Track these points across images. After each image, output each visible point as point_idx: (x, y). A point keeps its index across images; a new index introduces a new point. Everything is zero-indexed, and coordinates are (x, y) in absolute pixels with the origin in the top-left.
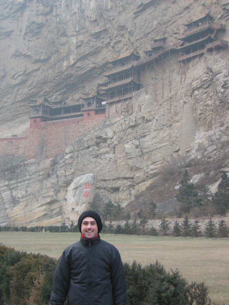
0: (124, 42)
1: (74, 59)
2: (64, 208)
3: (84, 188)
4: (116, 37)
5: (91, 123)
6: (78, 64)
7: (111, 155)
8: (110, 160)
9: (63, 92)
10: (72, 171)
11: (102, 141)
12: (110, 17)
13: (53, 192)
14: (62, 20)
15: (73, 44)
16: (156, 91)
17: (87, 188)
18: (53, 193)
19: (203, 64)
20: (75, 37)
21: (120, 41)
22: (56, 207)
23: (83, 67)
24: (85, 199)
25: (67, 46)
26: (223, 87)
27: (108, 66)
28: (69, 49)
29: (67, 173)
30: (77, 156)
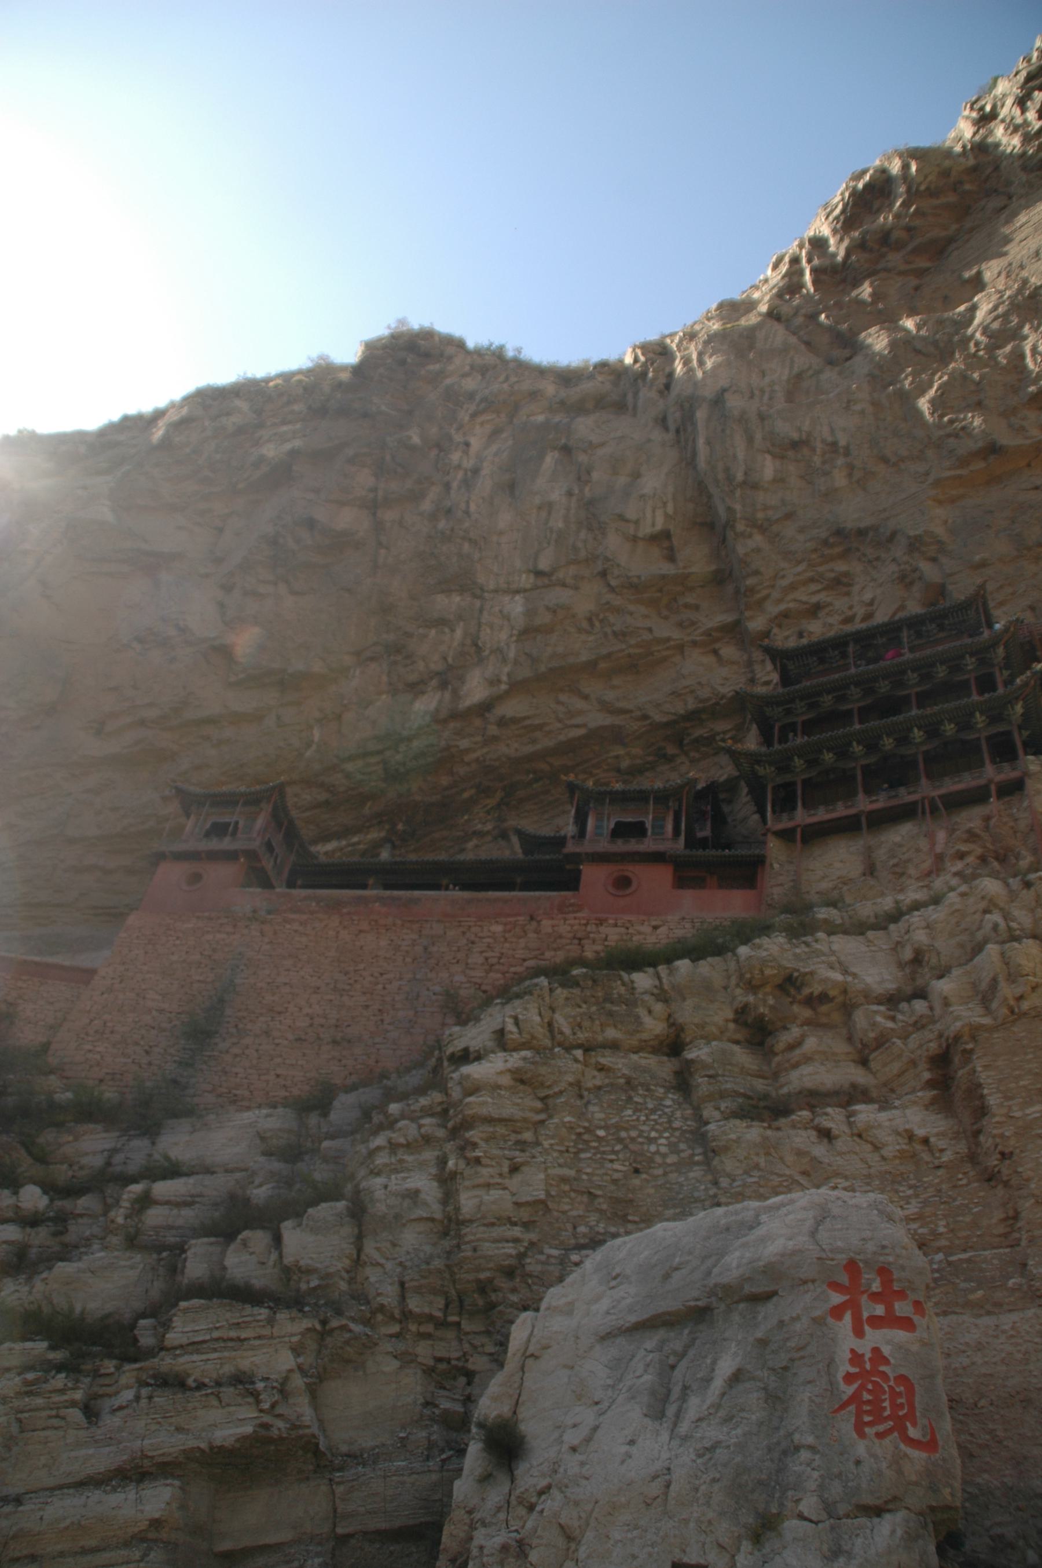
0: (851, 608)
3: (837, 1312)
4: (793, 587)
5: (646, 929)
6: (511, 708)
8: (902, 1155)
9: (361, 846)
11: (807, 1013)
12: (766, 508)
13: (297, 1350)
14: (467, 524)
15: (507, 618)
17: (876, 1322)
18: (286, 1361)
20: (517, 598)
21: (814, 611)
22: (284, 1536)
23: (537, 722)
25: (459, 633)
27: (699, 732)
28: (468, 641)
29: (467, 1202)
30: (578, 1084)
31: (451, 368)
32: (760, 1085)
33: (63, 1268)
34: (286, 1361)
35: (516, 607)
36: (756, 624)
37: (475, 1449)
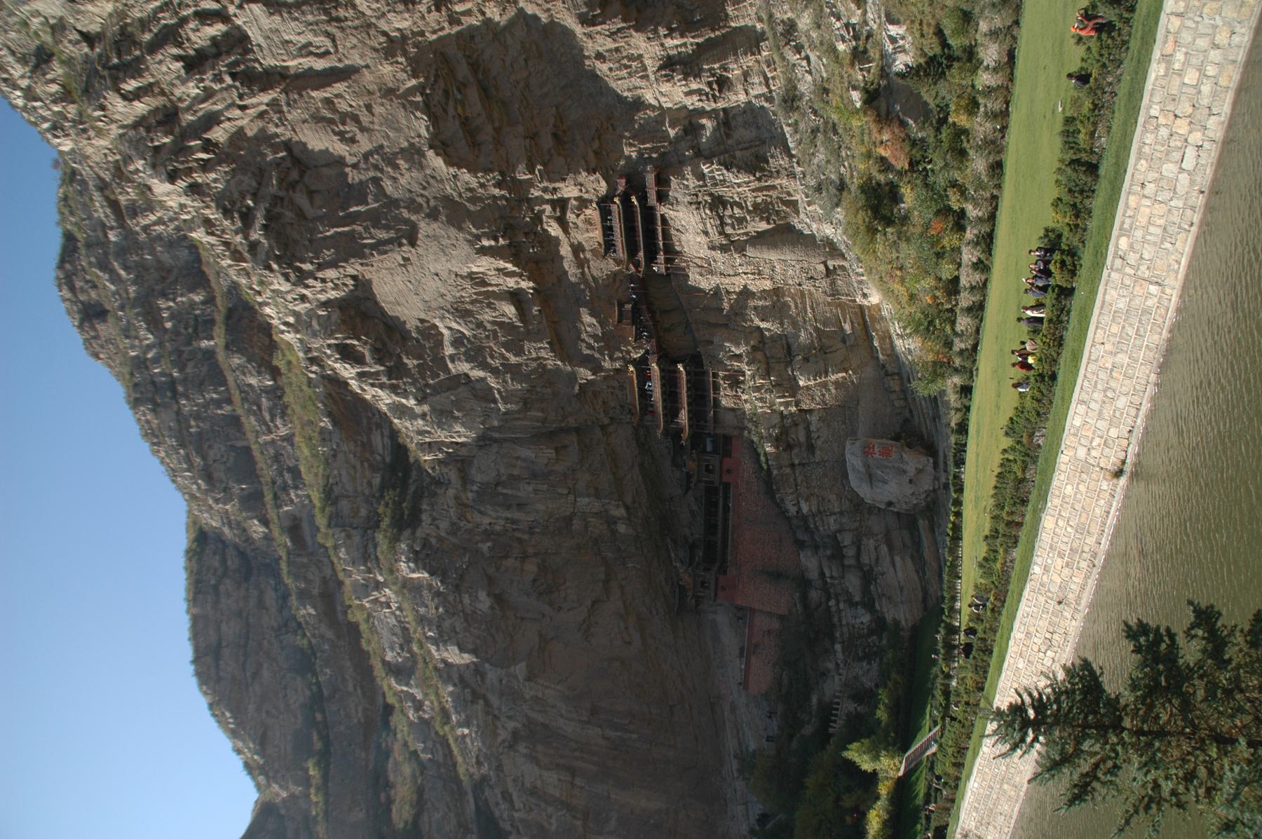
1: (618, 506)
2: (904, 506)
4: (594, 409)
6: (629, 500)
7: (814, 419)
10: (833, 497)
11: (784, 437)
16: (709, 324)
18: (871, 541)
19: (681, 214)
20: (578, 499)
21: (604, 402)
24: (894, 456)
25: (592, 520)
26: (728, 170)
29: (837, 510)
30: (807, 488)
31: (434, 534)
32: (803, 448)
33: (851, 590)
34: (871, 541)
35: (583, 501)
36: (606, 421)
37: (892, 509)
